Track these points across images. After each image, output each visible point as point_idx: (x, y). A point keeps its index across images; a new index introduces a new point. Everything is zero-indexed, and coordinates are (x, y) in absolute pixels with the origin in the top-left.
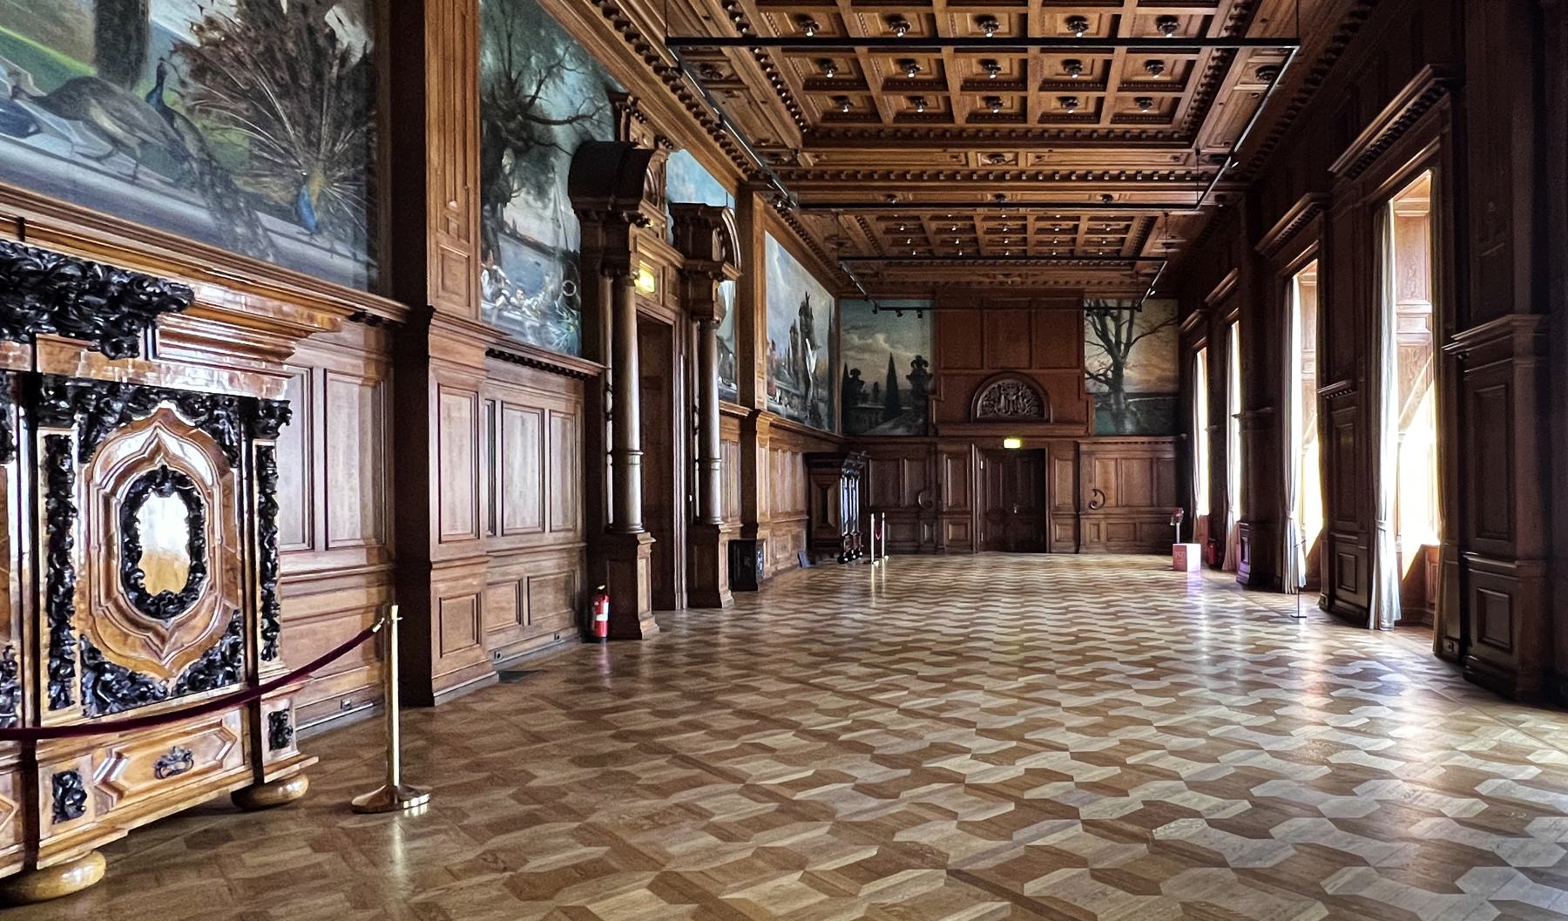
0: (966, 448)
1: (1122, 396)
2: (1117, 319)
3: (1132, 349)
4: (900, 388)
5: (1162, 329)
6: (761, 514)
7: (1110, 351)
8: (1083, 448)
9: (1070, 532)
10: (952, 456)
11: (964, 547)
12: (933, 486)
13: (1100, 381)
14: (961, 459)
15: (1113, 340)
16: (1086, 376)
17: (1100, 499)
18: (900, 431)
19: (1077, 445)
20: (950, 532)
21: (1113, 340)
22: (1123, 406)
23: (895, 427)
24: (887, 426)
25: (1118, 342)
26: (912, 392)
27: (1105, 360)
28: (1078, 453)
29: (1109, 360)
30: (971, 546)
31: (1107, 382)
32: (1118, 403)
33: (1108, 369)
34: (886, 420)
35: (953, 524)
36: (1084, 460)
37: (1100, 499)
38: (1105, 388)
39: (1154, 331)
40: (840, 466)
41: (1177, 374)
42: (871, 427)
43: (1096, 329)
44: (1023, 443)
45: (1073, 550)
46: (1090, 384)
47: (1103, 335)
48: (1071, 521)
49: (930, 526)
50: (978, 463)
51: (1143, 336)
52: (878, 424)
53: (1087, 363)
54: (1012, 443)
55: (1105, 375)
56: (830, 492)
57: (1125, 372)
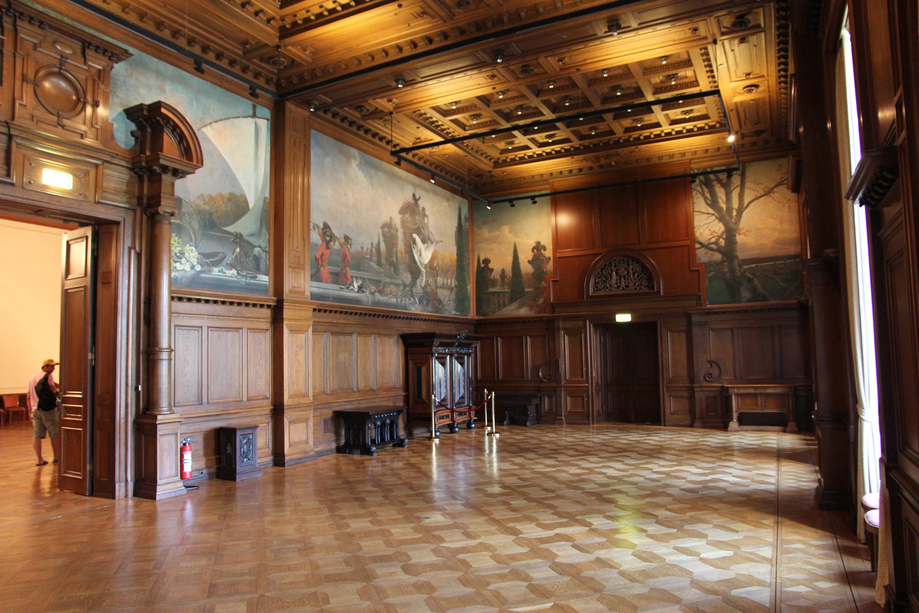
0: (581, 323)
1: (736, 262)
2: (726, 186)
3: (745, 214)
4: (523, 272)
5: (775, 190)
6: (291, 397)
7: (721, 219)
8: (695, 318)
9: (685, 404)
10: (570, 332)
11: (580, 419)
12: (552, 362)
13: (712, 249)
14: (576, 334)
15: (724, 206)
16: (697, 246)
17: (715, 371)
18: (524, 312)
19: (689, 317)
20: (567, 403)
21: (724, 206)
22: (738, 274)
23: (520, 307)
24: (514, 306)
25: (729, 209)
26: (533, 274)
27: (717, 230)
28: (690, 324)
29: (720, 228)
30: (588, 417)
31: (719, 250)
32: (732, 270)
33: (719, 237)
34: (512, 301)
35: (570, 397)
36: (696, 331)
37: (715, 371)
38: (718, 257)
39: (768, 192)
40: (431, 346)
41: (799, 235)
42: (499, 309)
43: (705, 199)
44: (632, 318)
45: (688, 422)
46: (702, 256)
47: (714, 204)
48: (686, 394)
49: (550, 397)
50: (593, 340)
51: (757, 198)
52: (505, 306)
53: (697, 234)
54: (623, 318)
55: (715, 243)
56: (424, 369)
57: (739, 238)
